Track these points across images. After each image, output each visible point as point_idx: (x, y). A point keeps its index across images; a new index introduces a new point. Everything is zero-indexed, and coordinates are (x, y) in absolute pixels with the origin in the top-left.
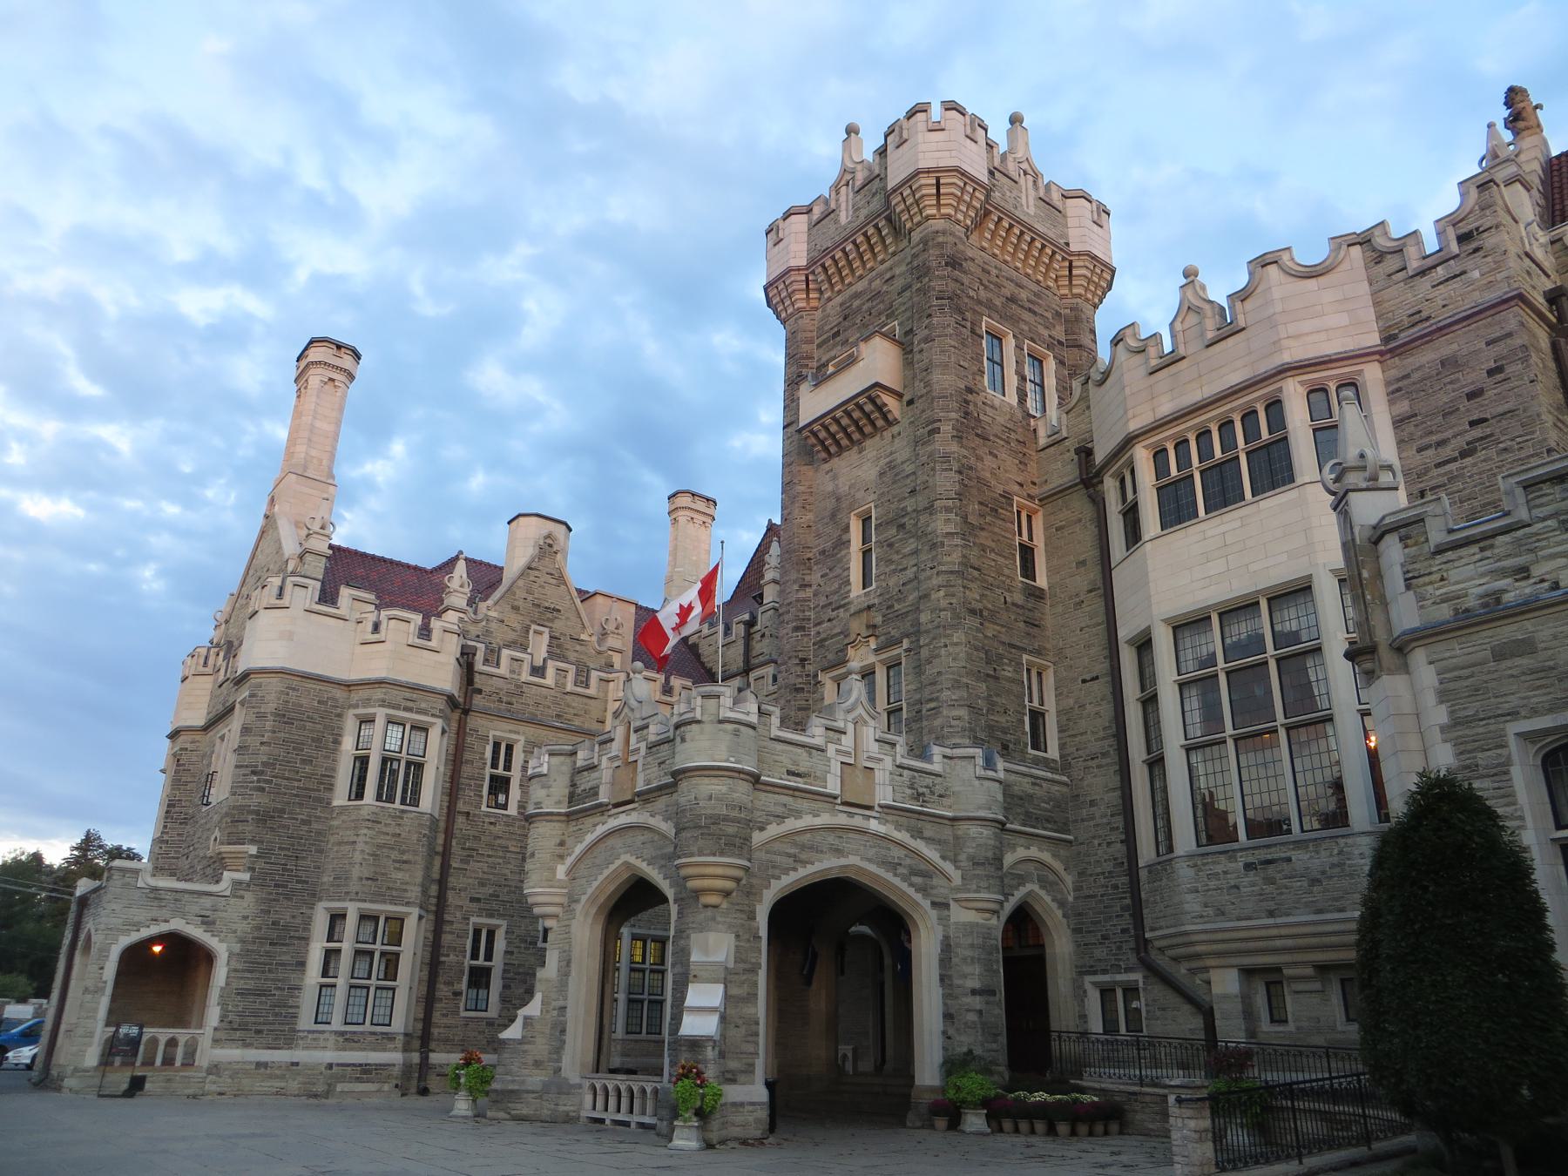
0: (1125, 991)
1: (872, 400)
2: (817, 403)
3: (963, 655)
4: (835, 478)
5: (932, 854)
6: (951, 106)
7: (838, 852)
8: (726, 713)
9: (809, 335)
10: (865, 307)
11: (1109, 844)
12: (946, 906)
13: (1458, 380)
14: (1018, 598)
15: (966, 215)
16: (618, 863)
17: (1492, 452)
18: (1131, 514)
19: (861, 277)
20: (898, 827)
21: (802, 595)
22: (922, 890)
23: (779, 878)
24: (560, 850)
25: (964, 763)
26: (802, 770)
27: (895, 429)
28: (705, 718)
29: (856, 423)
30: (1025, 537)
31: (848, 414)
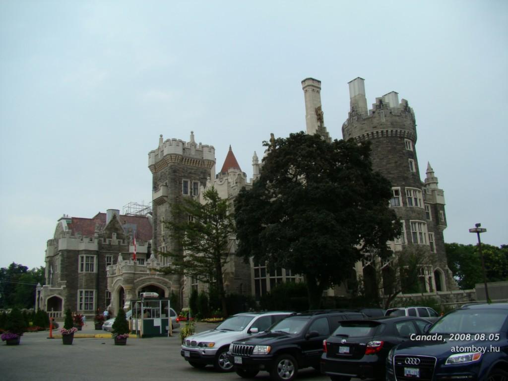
7: (150, 281)
12: (170, 288)
20: (161, 276)
22: (165, 286)
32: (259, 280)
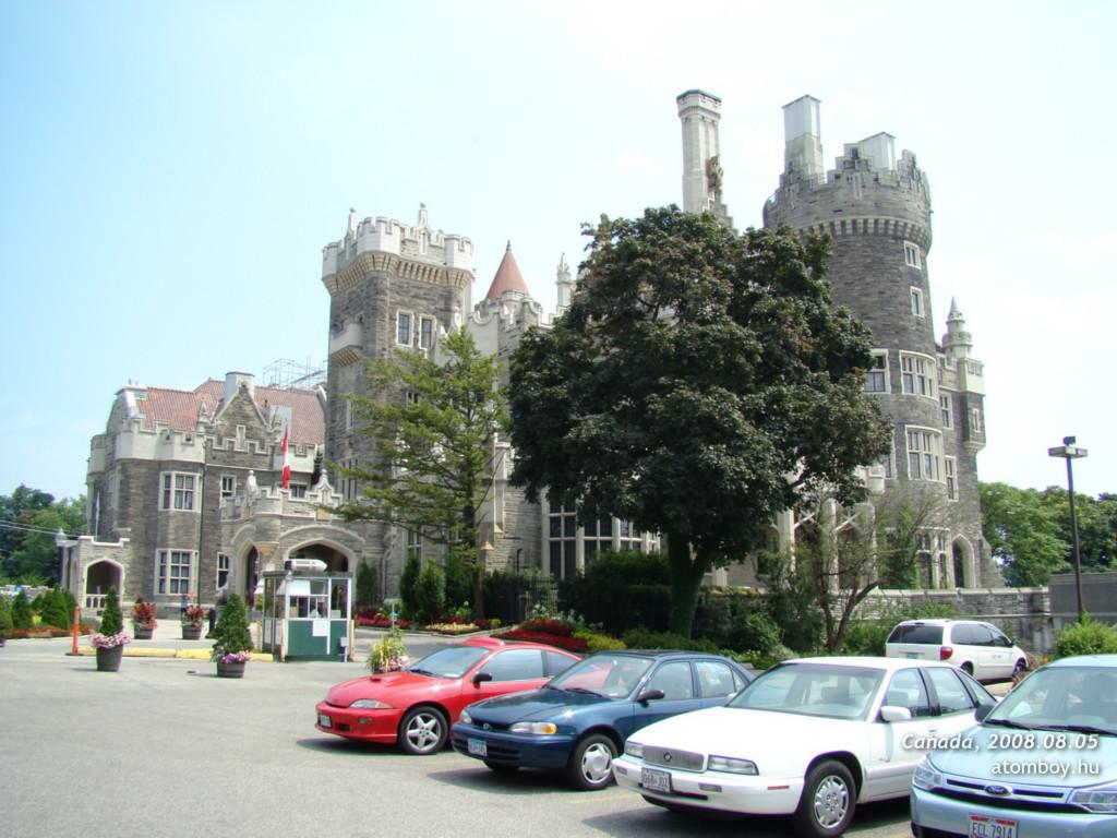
7: (315, 536)
8: (269, 496)
20: (340, 526)
22: (350, 547)
32: (558, 543)
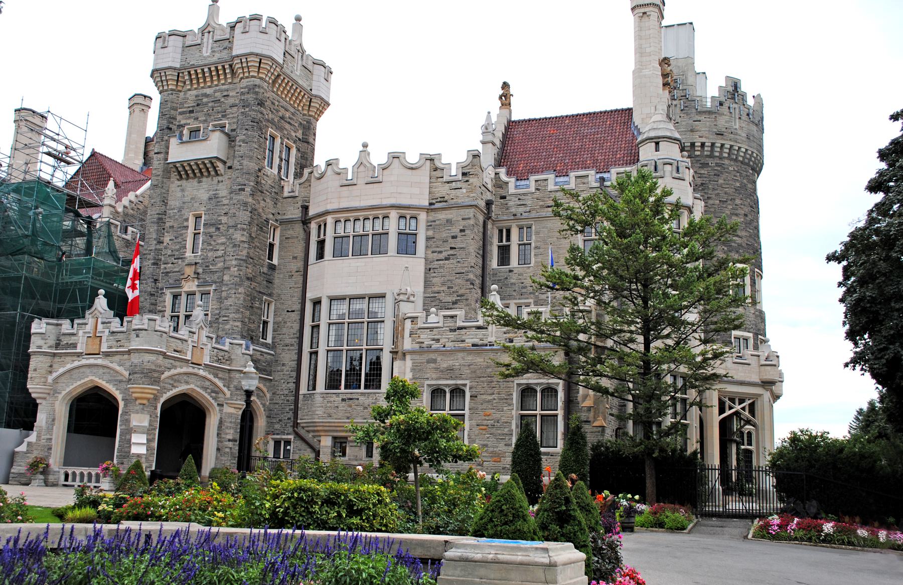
0: (285, 442)
1: (212, 163)
2: (179, 152)
3: (242, 298)
4: (183, 190)
5: (220, 384)
6: (273, 22)
7: (187, 383)
9: (175, 105)
10: (210, 105)
11: (288, 383)
12: (222, 405)
13: (450, 230)
14: (265, 270)
15: (270, 78)
16: (86, 380)
17: (455, 261)
18: (321, 244)
19: (210, 87)
21: (158, 247)
22: (215, 399)
23: (166, 393)
24: (49, 369)
25: (238, 347)
26: (179, 349)
27: (220, 178)
28: (149, 329)
29: (200, 170)
30: (271, 240)
31: (197, 165)
